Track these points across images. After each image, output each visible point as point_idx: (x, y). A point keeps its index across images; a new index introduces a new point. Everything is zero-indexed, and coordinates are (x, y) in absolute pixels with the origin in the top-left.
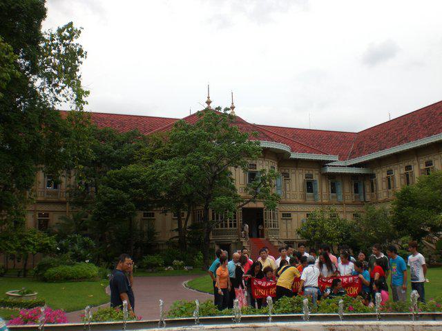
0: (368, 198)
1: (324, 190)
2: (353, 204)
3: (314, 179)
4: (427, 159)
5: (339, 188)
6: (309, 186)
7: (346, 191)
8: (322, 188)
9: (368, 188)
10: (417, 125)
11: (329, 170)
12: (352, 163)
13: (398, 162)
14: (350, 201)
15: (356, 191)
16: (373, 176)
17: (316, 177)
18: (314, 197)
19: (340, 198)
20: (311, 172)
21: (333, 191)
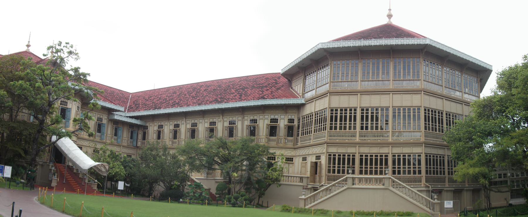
0: (139, 144)
1: (109, 132)
2: (127, 147)
3: (103, 122)
4: (193, 121)
5: (120, 133)
6: (99, 127)
7: (125, 134)
8: (109, 130)
9: (140, 136)
10: (185, 95)
11: (117, 117)
12: (131, 115)
13: (169, 120)
14: (126, 144)
15: (131, 138)
16: (146, 128)
17: (105, 121)
18: (101, 137)
19: (119, 140)
20: (101, 117)
21: (116, 135)
